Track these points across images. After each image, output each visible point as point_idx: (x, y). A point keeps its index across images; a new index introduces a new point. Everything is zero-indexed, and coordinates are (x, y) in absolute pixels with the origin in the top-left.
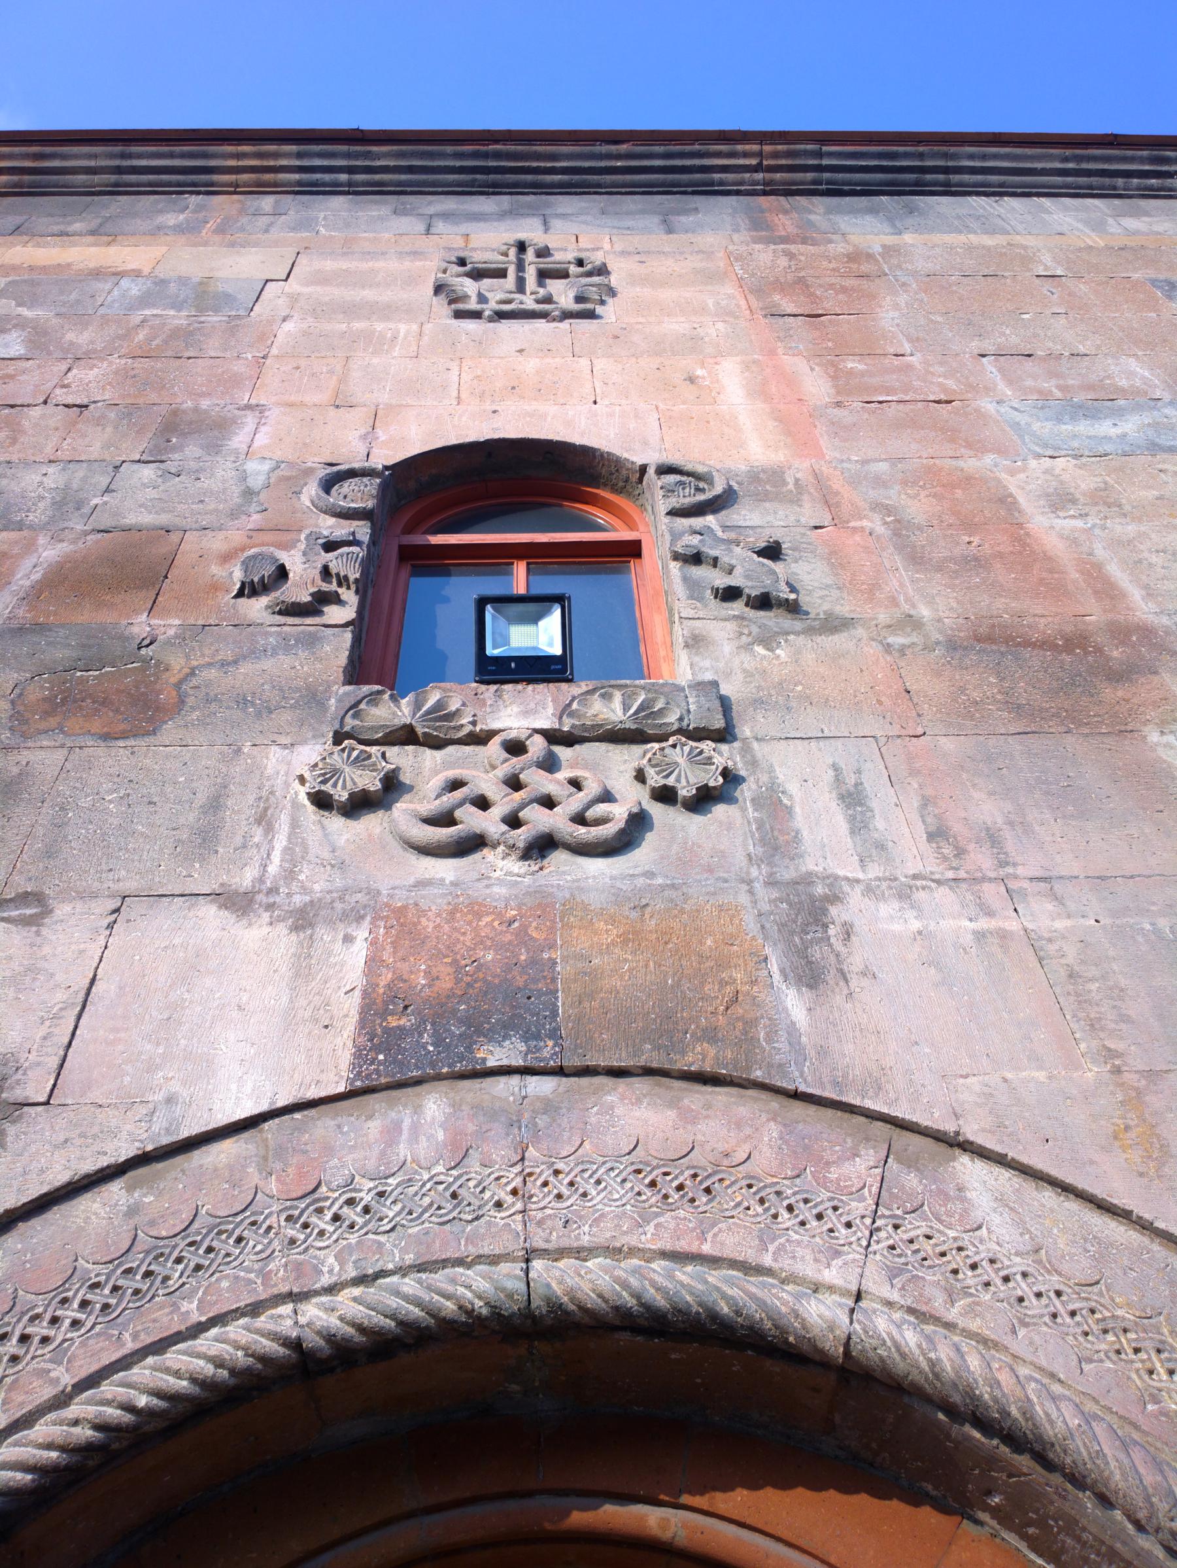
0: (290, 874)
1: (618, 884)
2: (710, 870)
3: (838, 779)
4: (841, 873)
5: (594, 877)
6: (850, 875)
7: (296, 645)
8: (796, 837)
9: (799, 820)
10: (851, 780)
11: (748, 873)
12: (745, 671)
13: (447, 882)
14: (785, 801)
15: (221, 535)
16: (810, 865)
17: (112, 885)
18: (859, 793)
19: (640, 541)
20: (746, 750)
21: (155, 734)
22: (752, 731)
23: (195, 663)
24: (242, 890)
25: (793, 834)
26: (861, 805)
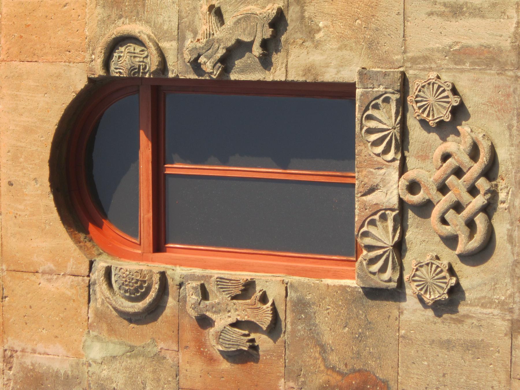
0: (502, 304)
1: (515, 142)
2: (508, 96)
3: (441, 15)
4: (512, 30)
5: (511, 154)
6: (514, 25)
7: (306, 314)
8: (485, 47)
9: (474, 43)
10: (443, 9)
11: (512, 77)
12: (340, 49)
13: (510, 228)
14: (457, 47)
15: (184, 367)
16: (507, 44)
17: (503, 385)
18: (452, 7)
19: (151, 86)
20: (414, 60)
21: (387, 382)
22: (397, 55)
23: (322, 368)
24: (510, 325)
25: (483, 48)
26: (461, 7)
